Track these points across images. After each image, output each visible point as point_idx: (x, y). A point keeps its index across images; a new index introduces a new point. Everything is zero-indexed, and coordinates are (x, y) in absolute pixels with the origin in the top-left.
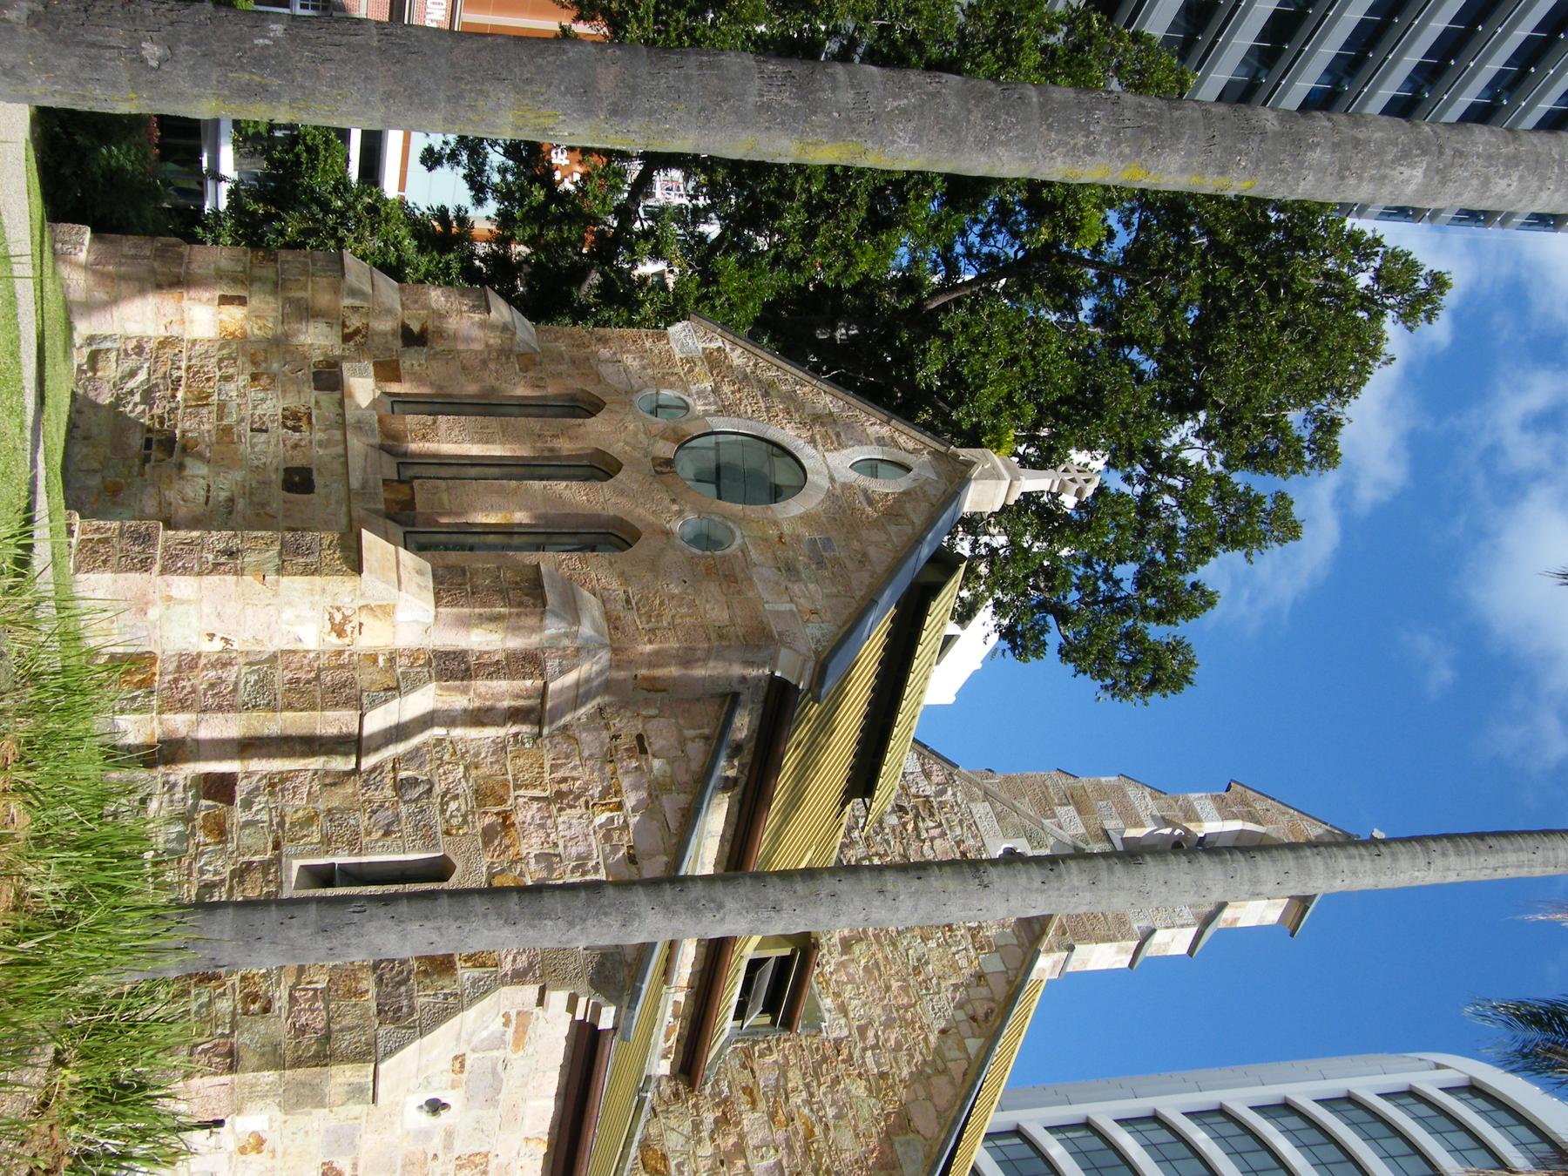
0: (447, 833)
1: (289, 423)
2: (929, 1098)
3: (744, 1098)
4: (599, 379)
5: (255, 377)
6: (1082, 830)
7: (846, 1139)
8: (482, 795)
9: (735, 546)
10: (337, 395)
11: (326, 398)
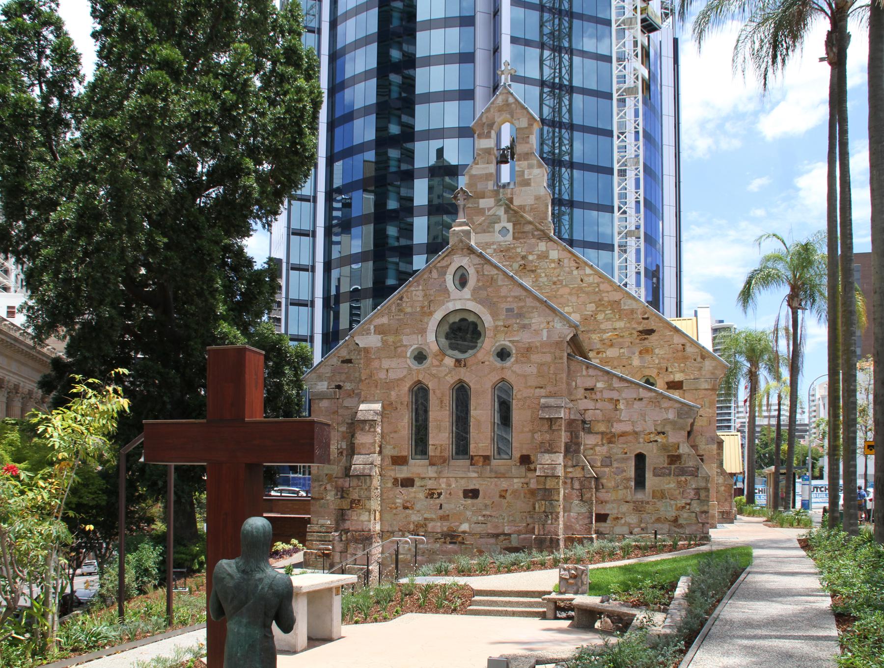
0: (626, 453)
1: (435, 496)
2: (608, 292)
3: (600, 355)
4: (401, 380)
5: (405, 508)
6: (493, 200)
7: (620, 324)
8: (610, 442)
9: (510, 345)
10: (416, 480)
11: (418, 483)
